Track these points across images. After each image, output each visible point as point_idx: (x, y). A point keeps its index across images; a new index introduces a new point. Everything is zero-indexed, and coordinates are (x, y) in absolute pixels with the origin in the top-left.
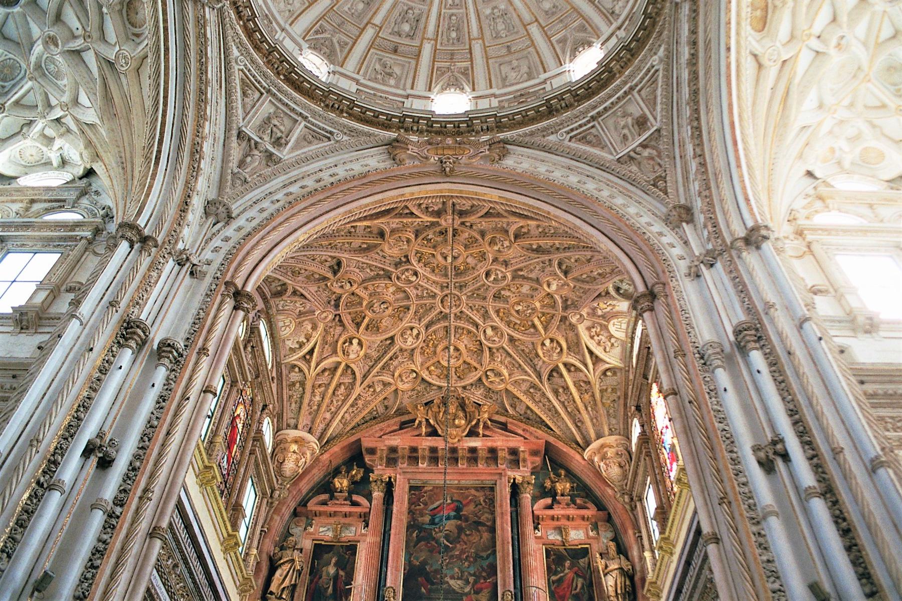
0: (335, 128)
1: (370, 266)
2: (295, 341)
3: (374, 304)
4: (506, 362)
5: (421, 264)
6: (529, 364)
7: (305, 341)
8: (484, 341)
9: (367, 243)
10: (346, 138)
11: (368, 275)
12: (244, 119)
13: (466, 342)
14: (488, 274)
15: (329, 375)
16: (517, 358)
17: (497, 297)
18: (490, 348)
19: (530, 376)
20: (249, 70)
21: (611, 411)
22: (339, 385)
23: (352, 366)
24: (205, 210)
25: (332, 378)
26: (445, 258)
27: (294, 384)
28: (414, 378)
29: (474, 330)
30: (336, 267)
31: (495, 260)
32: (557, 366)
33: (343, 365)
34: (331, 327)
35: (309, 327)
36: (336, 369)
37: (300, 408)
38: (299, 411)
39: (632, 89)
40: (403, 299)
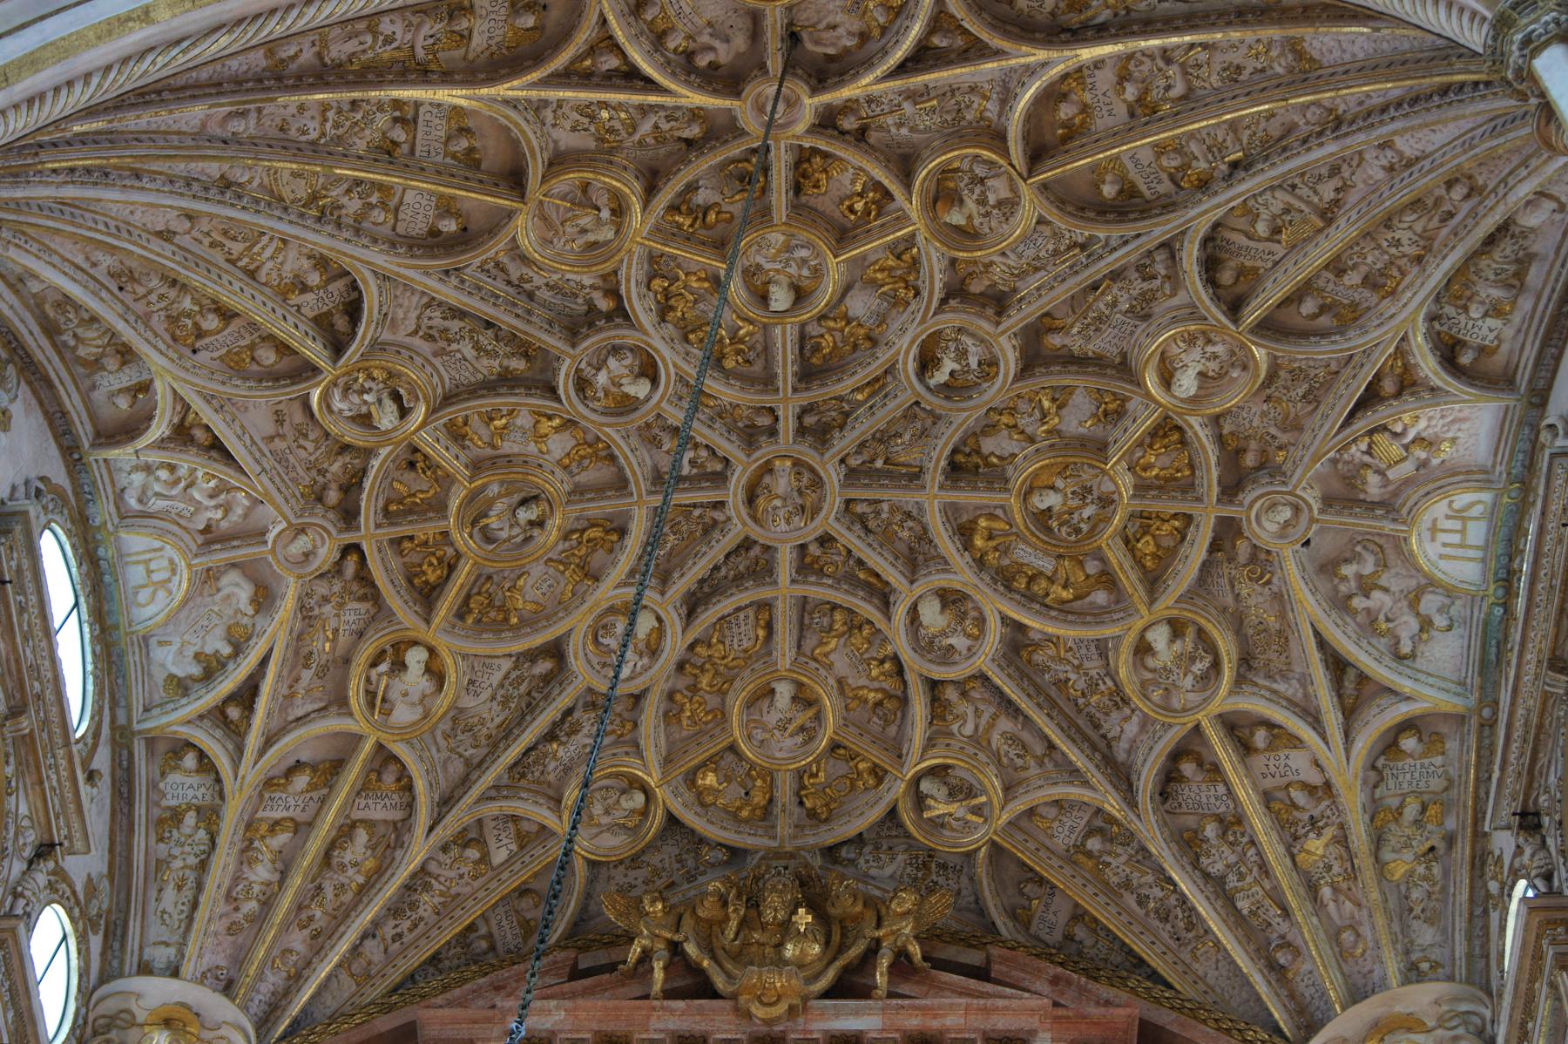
4: (996, 738)
5: (670, 329)
6: (1086, 738)
8: (907, 655)
13: (841, 664)
15: (312, 787)
16: (1039, 718)
17: (959, 469)
18: (934, 686)
19: (1086, 784)
21: (1416, 894)
22: (346, 831)
23: (400, 750)
25: (323, 801)
27: (176, 816)
28: (645, 813)
29: (868, 610)
32: (1197, 729)
33: (367, 747)
34: (326, 600)
36: (337, 766)
37: (195, 905)
38: (190, 919)
40: (599, 490)
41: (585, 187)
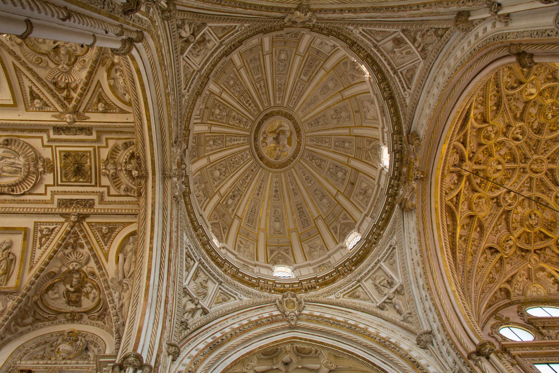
0: (388, 243)
1: (496, 225)
2: (552, 285)
3: (530, 224)
7: (553, 278)
9: (476, 228)
10: (395, 237)
11: (505, 227)
12: (373, 302)
14: (517, 139)
20: (345, 291)
24: (422, 348)
26: (499, 170)
30: (493, 250)
31: (505, 134)
35: (541, 274)
39: (375, 46)
41: (475, 204)
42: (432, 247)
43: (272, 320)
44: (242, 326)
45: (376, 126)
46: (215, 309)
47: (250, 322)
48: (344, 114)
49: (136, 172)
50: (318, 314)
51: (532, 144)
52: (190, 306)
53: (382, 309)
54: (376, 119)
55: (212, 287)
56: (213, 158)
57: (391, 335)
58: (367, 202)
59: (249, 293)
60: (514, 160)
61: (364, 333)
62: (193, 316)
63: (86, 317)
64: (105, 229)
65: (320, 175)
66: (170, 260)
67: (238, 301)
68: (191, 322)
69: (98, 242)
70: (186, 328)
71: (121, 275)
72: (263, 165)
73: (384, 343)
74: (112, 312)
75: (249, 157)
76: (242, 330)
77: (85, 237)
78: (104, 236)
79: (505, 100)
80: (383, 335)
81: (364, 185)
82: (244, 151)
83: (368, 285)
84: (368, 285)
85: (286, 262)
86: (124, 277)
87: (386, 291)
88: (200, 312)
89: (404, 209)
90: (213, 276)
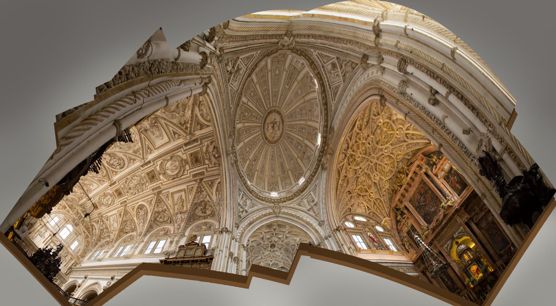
42: (330, 187)
43: (270, 214)
44: (260, 216)
45: (317, 121)
46: (250, 210)
47: (262, 215)
48: (304, 112)
49: (217, 155)
50: (286, 212)
51: (374, 148)
52: (241, 210)
53: (309, 211)
54: (318, 116)
55: (248, 202)
56: (246, 141)
57: (310, 221)
58: (309, 163)
59: (262, 203)
60: (365, 154)
61: (301, 219)
62: (242, 213)
63: (209, 217)
64: (210, 183)
65: (291, 147)
66: (233, 192)
67: (258, 207)
68: (242, 215)
69: (208, 189)
70: (241, 218)
71: (218, 200)
72: (267, 142)
73: (308, 223)
74: (216, 214)
75: (261, 138)
76: (260, 218)
77: (203, 187)
78: (210, 186)
79: (371, 120)
80: (308, 220)
81: (309, 154)
82: (259, 135)
83: (305, 201)
84: (305, 201)
85: (276, 190)
86: (220, 201)
87: (311, 204)
88: (245, 212)
89: (323, 168)
90: (248, 197)
